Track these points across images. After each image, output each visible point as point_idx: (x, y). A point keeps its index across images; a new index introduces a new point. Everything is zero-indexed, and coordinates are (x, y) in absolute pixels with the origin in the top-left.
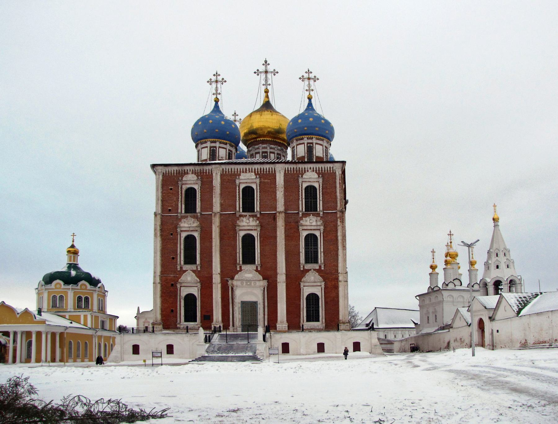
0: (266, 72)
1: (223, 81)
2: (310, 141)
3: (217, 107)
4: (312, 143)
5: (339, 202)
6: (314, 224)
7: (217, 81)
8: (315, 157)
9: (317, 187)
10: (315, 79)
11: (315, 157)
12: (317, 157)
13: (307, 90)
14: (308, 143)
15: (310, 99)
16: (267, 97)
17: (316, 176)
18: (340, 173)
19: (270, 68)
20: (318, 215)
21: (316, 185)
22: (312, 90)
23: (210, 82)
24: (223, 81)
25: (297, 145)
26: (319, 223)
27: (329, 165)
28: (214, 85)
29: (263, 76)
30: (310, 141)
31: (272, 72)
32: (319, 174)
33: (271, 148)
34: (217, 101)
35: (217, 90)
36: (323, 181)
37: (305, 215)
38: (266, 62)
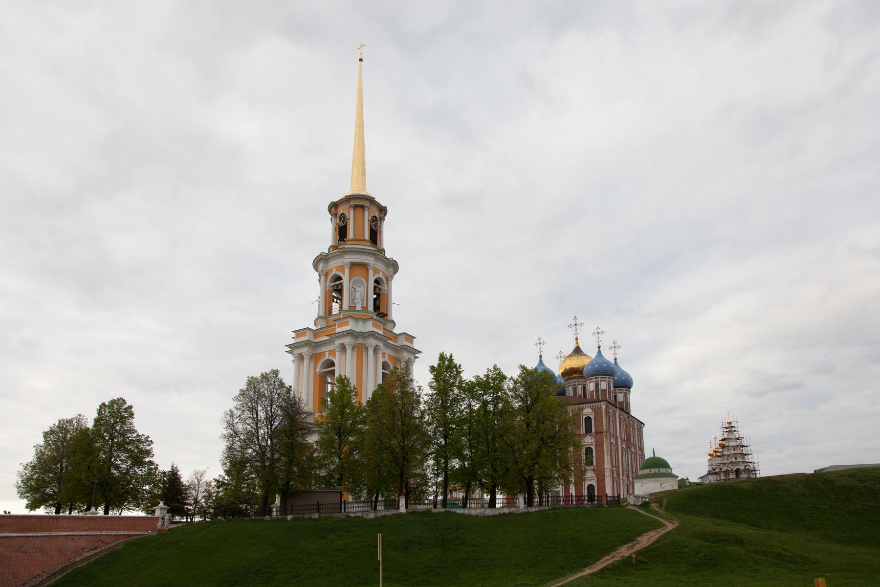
0: (576, 325)
1: (544, 342)
2: (597, 380)
3: (541, 361)
4: (598, 381)
5: (604, 426)
6: (590, 441)
7: (540, 344)
8: (600, 390)
9: (592, 418)
10: (602, 333)
11: (600, 390)
12: (602, 390)
13: (597, 342)
14: (595, 382)
15: (599, 347)
16: (577, 343)
17: (591, 411)
18: (605, 407)
19: (578, 322)
20: (592, 435)
21: (591, 416)
22: (601, 341)
23: (536, 344)
24: (544, 342)
25: (590, 383)
26: (593, 440)
27: (598, 403)
28: (538, 346)
29: (574, 327)
30: (597, 380)
31: (579, 324)
32: (592, 409)
33: (578, 382)
34: (541, 357)
35: (540, 350)
36: (595, 413)
37: (585, 436)
38: (575, 317)
